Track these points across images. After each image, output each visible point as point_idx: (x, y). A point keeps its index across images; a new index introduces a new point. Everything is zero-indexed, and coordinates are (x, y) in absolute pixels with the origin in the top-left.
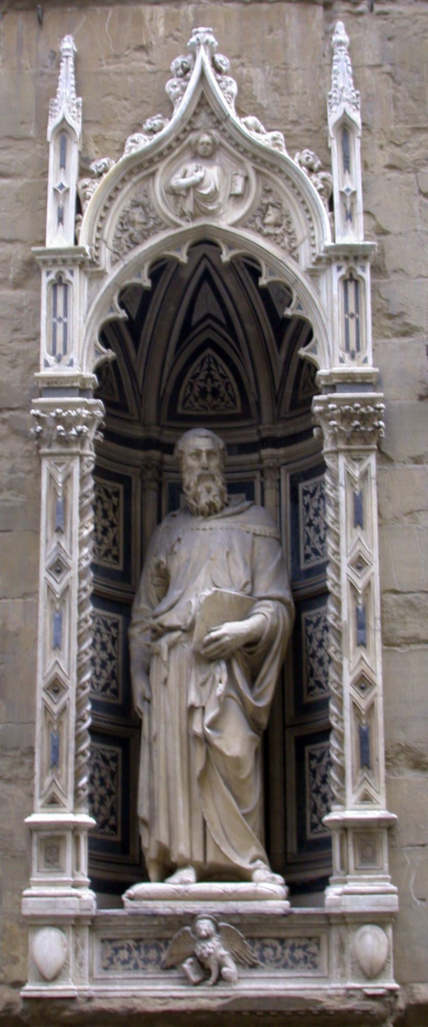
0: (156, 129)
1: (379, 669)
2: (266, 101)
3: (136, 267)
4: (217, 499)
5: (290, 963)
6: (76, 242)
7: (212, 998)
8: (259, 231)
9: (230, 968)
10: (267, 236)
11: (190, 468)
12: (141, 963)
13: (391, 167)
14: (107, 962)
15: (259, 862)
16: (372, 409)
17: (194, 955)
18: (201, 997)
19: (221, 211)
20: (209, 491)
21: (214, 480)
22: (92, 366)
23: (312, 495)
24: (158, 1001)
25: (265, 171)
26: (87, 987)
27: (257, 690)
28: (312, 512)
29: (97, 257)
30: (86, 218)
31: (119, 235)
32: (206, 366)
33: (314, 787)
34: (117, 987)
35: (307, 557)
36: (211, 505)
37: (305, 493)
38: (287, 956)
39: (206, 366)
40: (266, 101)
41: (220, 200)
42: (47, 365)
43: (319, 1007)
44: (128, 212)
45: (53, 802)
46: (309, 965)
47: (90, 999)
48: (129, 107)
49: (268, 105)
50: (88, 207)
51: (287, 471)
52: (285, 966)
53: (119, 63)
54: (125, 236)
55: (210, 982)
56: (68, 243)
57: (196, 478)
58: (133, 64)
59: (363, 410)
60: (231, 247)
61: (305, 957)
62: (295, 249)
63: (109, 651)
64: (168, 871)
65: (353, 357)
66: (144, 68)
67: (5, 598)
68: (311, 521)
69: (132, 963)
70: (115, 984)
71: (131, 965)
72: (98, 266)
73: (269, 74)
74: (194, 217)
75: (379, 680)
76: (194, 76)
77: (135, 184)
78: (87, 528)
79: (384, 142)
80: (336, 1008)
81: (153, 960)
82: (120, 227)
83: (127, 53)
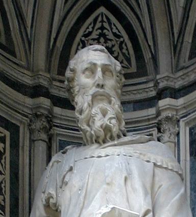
4: (114, 121)
11: (84, 87)
20: (104, 113)
21: (110, 102)
32: (98, 25)
36: (107, 129)
39: (98, 25)
51: (187, 124)
57: (90, 98)
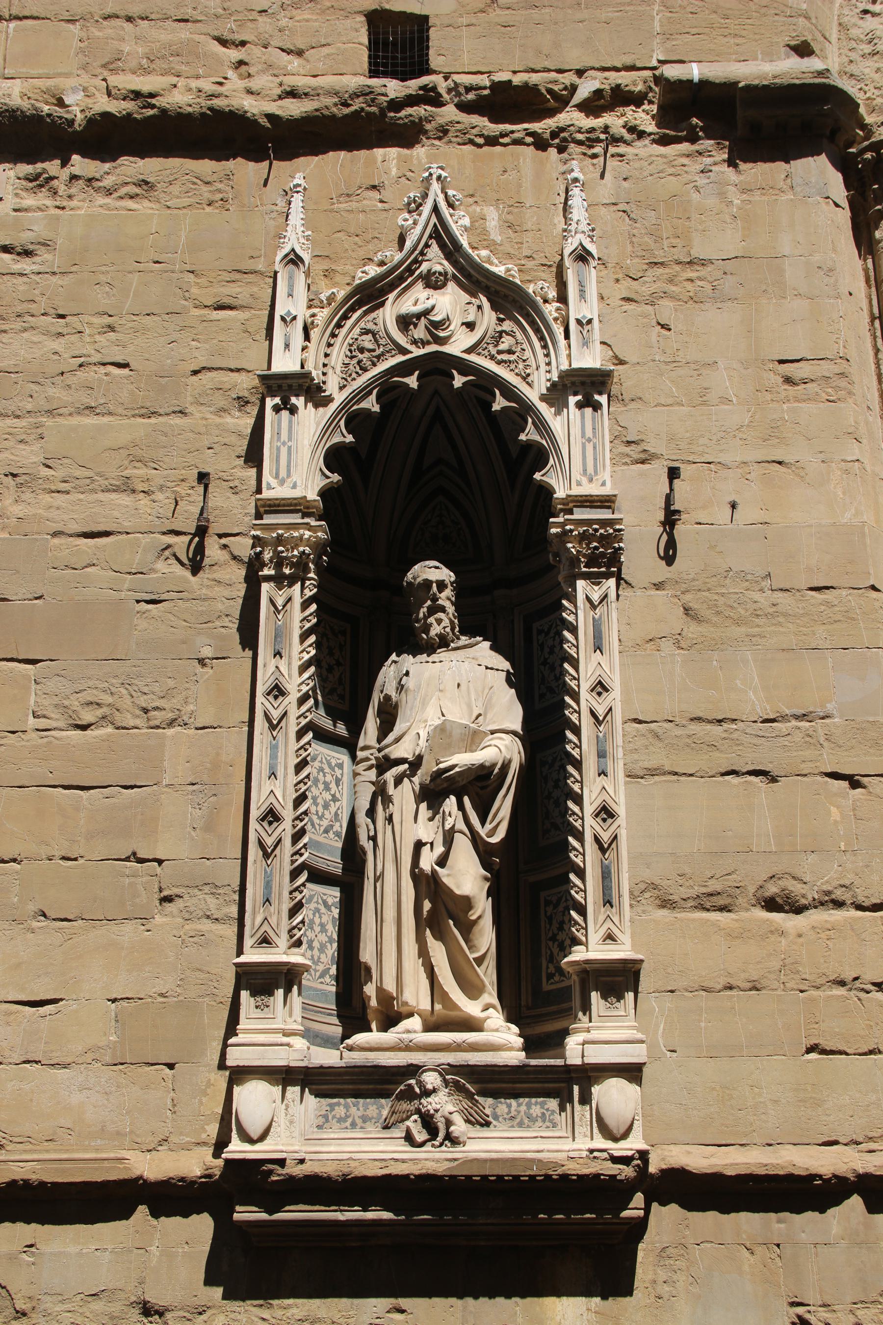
0: (386, 261)
1: (622, 799)
2: (500, 238)
3: (363, 393)
5: (526, 1121)
6: (302, 367)
7: (438, 1161)
8: (492, 358)
9: (459, 1127)
10: (499, 363)
12: (359, 1122)
13: (628, 300)
14: (321, 1120)
15: (491, 1010)
16: (611, 531)
17: (418, 1111)
18: (426, 1160)
19: (452, 340)
22: (317, 490)
23: (547, 633)
24: (377, 1163)
25: (500, 301)
26: (296, 1148)
27: (489, 826)
28: (546, 650)
29: (324, 383)
30: (312, 346)
31: (347, 361)
33: (550, 934)
34: (332, 1149)
35: (542, 696)
37: (540, 632)
38: (522, 1113)
40: (500, 238)
41: (452, 328)
42: (270, 488)
43: (560, 1171)
44: (357, 339)
45: (265, 941)
46: (548, 1124)
47: (302, 1161)
48: (360, 243)
49: (502, 240)
50: (314, 334)
52: (521, 1125)
53: (351, 201)
54: (355, 361)
55: (437, 1143)
56: (295, 367)
58: (365, 202)
59: (602, 531)
60: (462, 373)
61: (543, 1114)
62: (528, 375)
63: (332, 793)
64: (390, 1020)
65: (591, 480)
66: (376, 206)
67: (220, 727)
68: (546, 659)
69: (350, 1120)
70: (330, 1145)
71: (348, 1124)
72: (325, 391)
73: (503, 212)
74: (424, 343)
75: (621, 809)
76: (427, 209)
77: (366, 313)
78: (308, 653)
79: (620, 276)
80: (580, 1173)
81: (373, 1118)
82: (349, 354)
83: (359, 192)
